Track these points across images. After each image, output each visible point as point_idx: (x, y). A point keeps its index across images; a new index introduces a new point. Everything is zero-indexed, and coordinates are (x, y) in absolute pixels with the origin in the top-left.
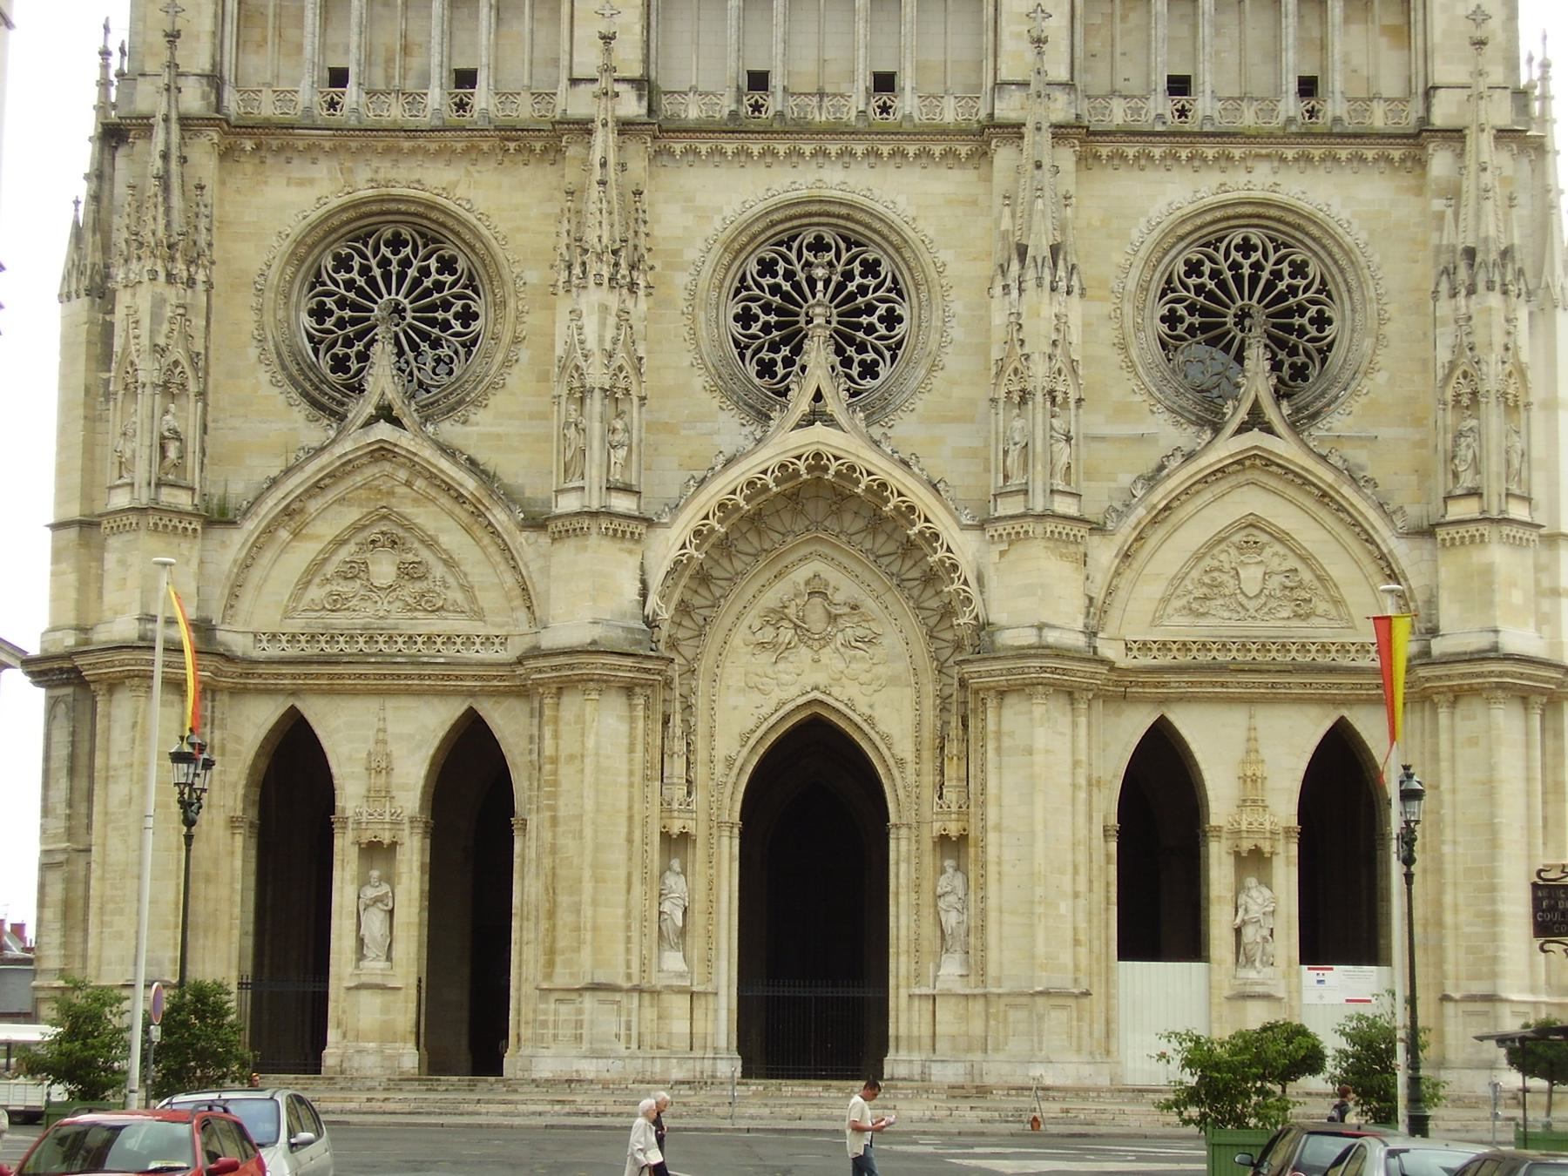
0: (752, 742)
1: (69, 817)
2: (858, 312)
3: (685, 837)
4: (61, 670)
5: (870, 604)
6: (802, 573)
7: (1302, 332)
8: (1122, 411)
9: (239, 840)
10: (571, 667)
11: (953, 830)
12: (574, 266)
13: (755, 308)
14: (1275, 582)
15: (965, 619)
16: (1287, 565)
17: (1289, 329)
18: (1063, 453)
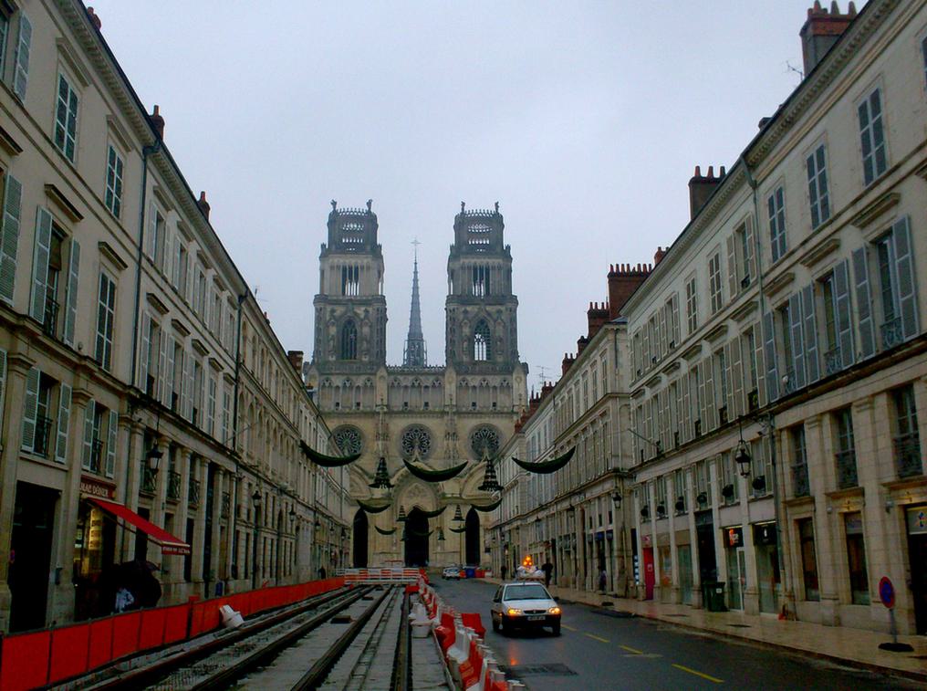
12: (377, 437)
15: (440, 493)
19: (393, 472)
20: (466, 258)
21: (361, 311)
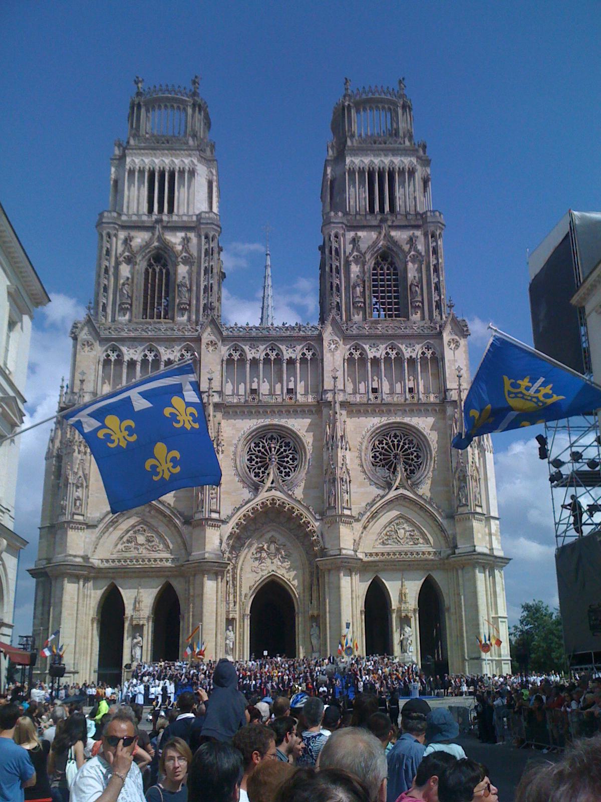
0: (253, 589)
1: (42, 619)
2: (284, 457)
3: (233, 619)
4: (41, 572)
5: (288, 544)
6: (268, 536)
7: (412, 460)
8: (361, 485)
9: (95, 625)
10: (198, 566)
11: (316, 613)
13: (253, 457)
14: (408, 533)
16: (411, 529)
17: (409, 459)
18: (346, 497)
19: (229, 513)
20: (356, 155)
21: (175, 239)
